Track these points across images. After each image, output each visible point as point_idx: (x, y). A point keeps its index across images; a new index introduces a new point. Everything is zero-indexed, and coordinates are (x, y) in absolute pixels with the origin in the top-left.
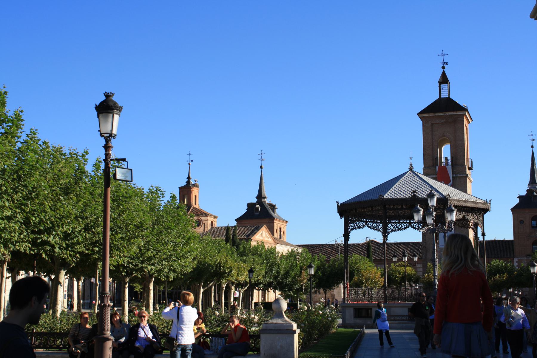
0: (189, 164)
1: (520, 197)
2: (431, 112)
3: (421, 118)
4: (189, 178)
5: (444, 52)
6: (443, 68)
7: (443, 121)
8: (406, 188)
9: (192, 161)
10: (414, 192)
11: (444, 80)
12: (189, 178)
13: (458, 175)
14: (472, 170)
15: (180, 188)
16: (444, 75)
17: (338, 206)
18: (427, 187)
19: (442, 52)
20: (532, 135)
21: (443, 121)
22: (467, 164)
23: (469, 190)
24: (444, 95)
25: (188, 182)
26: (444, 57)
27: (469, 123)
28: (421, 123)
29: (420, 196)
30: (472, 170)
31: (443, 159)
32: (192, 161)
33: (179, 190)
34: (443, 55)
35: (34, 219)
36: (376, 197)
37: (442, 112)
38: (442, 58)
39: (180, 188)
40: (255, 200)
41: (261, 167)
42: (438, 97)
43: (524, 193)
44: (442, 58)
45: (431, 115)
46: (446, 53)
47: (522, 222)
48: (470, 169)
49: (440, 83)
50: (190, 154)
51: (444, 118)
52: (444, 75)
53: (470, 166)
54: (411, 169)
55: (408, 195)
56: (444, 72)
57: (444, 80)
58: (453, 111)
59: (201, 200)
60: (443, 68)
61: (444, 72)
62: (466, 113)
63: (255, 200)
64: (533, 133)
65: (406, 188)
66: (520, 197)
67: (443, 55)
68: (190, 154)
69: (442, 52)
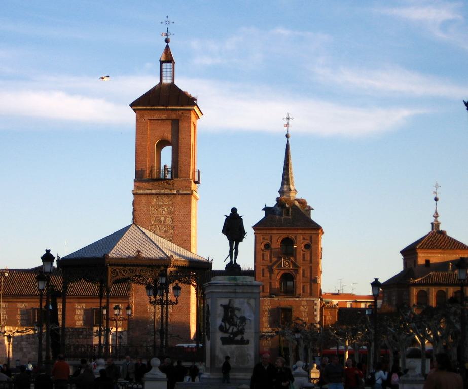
1: (266, 209)
2: (148, 105)
3: (135, 110)
8: (130, 245)
10: (139, 251)
11: (168, 59)
14: (199, 183)
18: (151, 245)
19: (166, 19)
20: (288, 119)
21: (163, 117)
22: (193, 177)
23: (193, 250)
24: (167, 80)
26: (169, 27)
29: (144, 256)
30: (199, 183)
31: (162, 168)
34: (167, 23)
35: (3, 323)
36: (99, 255)
37: (163, 106)
38: (166, 27)
42: (158, 82)
43: (272, 203)
44: (166, 27)
46: (171, 21)
47: (267, 246)
48: (196, 182)
49: (162, 62)
51: (167, 108)
53: (197, 180)
55: (133, 254)
56: (167, 47)
57: (168, 59)
58: (178, 105)
60: (167, 41)
61: (167, 47)
62: (195, 108)
64: (290, 116)
65: (130, 245)
66: (266, 209)
69: (166, 19)
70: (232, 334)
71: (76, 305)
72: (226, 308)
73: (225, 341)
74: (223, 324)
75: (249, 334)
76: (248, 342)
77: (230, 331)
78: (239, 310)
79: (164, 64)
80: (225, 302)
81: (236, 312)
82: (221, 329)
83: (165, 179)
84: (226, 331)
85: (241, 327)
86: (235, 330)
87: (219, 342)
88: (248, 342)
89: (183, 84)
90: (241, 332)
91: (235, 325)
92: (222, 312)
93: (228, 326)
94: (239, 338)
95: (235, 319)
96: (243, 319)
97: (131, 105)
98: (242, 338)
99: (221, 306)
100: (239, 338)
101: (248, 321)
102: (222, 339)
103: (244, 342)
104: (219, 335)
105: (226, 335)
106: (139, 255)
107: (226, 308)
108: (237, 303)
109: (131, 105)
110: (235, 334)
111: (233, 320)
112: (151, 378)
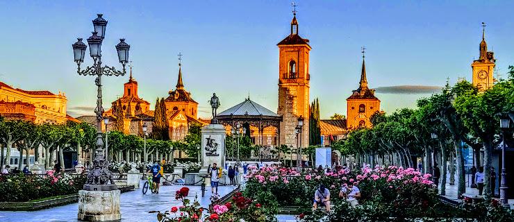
4: (131, 78)
11: (294, 23)
12: (131, 78)
16: (294, 19)
24: (294, 33)
25: (130, 80)
27: (309, 50)
45: (285, 46)
49: (292, 25)
57: (294, 23)
59: (141, 94)
60: (295, 14)
72: (208, 139)
82: (206, 149)
87: (205, 155)
89: (303, 36)
94: (214, 153)
96: (217, 144)
103: (216, 155)
110: (212, 151)
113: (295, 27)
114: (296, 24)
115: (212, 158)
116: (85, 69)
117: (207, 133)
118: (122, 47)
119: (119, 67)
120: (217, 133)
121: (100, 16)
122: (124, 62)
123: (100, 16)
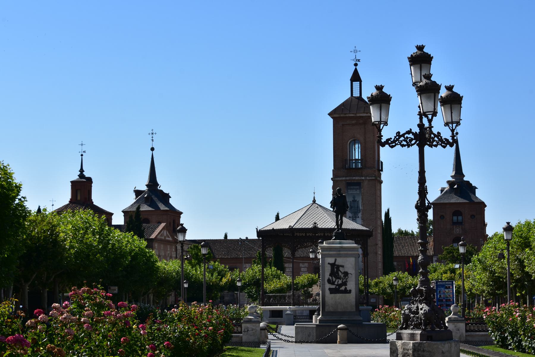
0: (82, 155)
3: (332, 118)
4: (82, 171)
5: (357, 49)
6: (356, 65)
7: (354, 122)
9: (84, 152)
11: (356, 77)
12: (82, 171)
13: (368, 178)
15: (72, 182)
16: (356, 71)
17: (257, 231)
19: (354, 48)
21: (354, 122)
24: (356, 94)
25: (82, 175)
26: (357, 54)
28: (332, 120)
32: (84, 152)
33: (70, 184)
34: (355, 51)
39: (72, 182)
40: (145, 188)
41: (152, 149)
42: (349, 96)
50: (82, 145)
52: (356, 71)
54: (314, 201)
55: (311, 226)
56: (356, 70)
57: (356, 77)
60: (356, 65)
61: (356, 70)
63: (145, 188)
67: (355, 51)
68: (82, 145)
69: (354, 48)
70: (337, 285)
71: (301, 265)
72: (333, 265)
73: (332, 291)
74: (331, 278)
75: (351, 285)
76: (350, 292)
77: (336, 283)
78: (343, 266)
79: (354, 83)
80: (331, 260)
81: (341, 269)
82: (329, 281)
83: (357, 169)
84: (333, 283)
85: (345, 280)
86: (340, 282)
87: (327, 292)
88: (350, 292)
90: (345, 284)
91: (340, 278)
92: (330, 269)
93: (334, 279)
94: (343, 288)
95: (340, 274)
96: (346, 274)
97: (329, 114)
98: (346, 288)
99: (329, 264)
100: (343, 288)
101: (349, 275)
102: (330, 289)
104: (328, 286)
105: (334, 287)
106: (315, 226)
107: (333, 265)
108: (339, 261)
109: (329, 114)
110: (340, 285)
111: (338, 275)
112: (336, 320)
113: (356, 84)
114: (360, 81)
115: (338, 296)
116: (392, 136)
117: (331, 256)
118: (454, 100)
119: (446, 134)
120: (347, 256)
121: (420, 48)
122: (453, 123)
123: (420, 48)
